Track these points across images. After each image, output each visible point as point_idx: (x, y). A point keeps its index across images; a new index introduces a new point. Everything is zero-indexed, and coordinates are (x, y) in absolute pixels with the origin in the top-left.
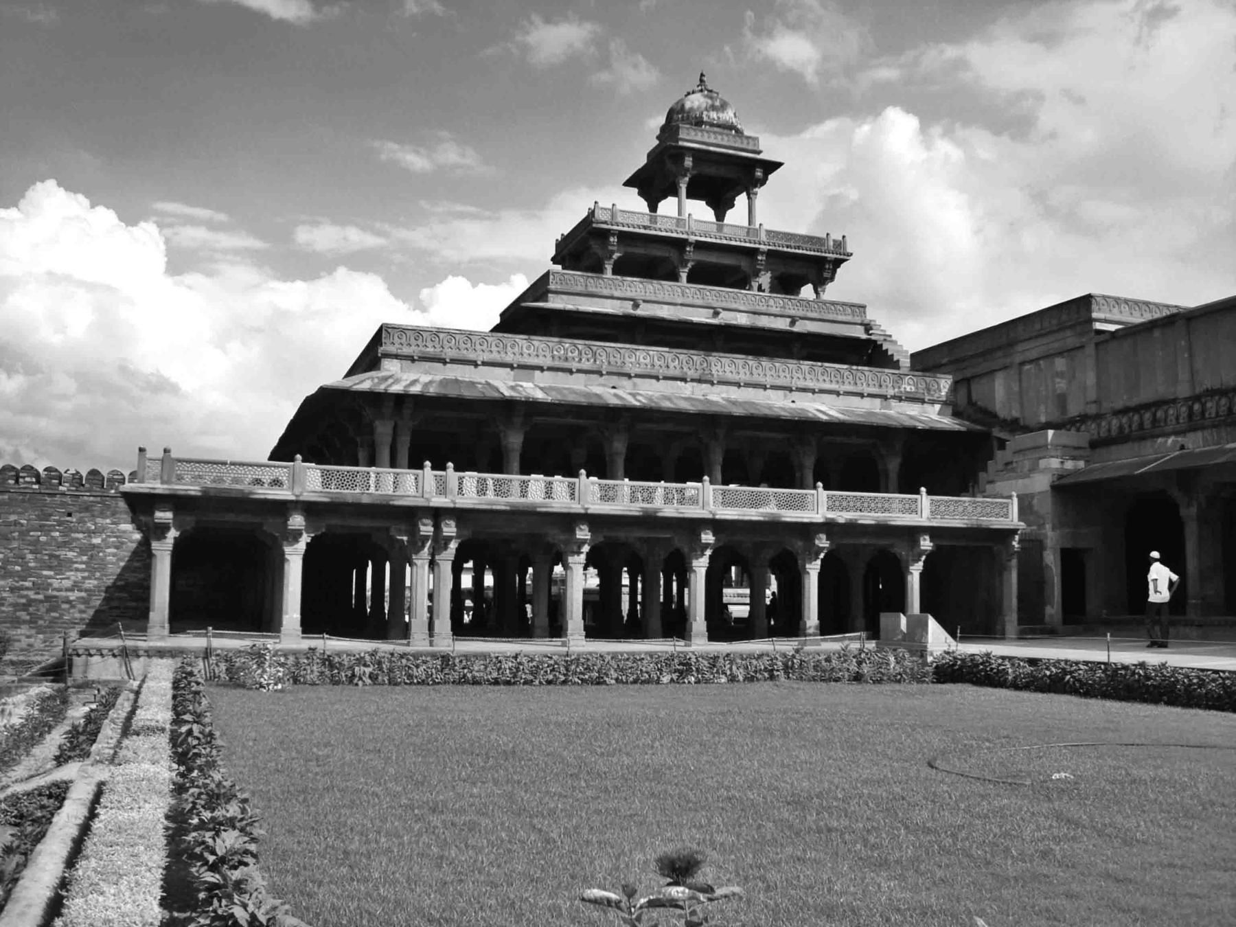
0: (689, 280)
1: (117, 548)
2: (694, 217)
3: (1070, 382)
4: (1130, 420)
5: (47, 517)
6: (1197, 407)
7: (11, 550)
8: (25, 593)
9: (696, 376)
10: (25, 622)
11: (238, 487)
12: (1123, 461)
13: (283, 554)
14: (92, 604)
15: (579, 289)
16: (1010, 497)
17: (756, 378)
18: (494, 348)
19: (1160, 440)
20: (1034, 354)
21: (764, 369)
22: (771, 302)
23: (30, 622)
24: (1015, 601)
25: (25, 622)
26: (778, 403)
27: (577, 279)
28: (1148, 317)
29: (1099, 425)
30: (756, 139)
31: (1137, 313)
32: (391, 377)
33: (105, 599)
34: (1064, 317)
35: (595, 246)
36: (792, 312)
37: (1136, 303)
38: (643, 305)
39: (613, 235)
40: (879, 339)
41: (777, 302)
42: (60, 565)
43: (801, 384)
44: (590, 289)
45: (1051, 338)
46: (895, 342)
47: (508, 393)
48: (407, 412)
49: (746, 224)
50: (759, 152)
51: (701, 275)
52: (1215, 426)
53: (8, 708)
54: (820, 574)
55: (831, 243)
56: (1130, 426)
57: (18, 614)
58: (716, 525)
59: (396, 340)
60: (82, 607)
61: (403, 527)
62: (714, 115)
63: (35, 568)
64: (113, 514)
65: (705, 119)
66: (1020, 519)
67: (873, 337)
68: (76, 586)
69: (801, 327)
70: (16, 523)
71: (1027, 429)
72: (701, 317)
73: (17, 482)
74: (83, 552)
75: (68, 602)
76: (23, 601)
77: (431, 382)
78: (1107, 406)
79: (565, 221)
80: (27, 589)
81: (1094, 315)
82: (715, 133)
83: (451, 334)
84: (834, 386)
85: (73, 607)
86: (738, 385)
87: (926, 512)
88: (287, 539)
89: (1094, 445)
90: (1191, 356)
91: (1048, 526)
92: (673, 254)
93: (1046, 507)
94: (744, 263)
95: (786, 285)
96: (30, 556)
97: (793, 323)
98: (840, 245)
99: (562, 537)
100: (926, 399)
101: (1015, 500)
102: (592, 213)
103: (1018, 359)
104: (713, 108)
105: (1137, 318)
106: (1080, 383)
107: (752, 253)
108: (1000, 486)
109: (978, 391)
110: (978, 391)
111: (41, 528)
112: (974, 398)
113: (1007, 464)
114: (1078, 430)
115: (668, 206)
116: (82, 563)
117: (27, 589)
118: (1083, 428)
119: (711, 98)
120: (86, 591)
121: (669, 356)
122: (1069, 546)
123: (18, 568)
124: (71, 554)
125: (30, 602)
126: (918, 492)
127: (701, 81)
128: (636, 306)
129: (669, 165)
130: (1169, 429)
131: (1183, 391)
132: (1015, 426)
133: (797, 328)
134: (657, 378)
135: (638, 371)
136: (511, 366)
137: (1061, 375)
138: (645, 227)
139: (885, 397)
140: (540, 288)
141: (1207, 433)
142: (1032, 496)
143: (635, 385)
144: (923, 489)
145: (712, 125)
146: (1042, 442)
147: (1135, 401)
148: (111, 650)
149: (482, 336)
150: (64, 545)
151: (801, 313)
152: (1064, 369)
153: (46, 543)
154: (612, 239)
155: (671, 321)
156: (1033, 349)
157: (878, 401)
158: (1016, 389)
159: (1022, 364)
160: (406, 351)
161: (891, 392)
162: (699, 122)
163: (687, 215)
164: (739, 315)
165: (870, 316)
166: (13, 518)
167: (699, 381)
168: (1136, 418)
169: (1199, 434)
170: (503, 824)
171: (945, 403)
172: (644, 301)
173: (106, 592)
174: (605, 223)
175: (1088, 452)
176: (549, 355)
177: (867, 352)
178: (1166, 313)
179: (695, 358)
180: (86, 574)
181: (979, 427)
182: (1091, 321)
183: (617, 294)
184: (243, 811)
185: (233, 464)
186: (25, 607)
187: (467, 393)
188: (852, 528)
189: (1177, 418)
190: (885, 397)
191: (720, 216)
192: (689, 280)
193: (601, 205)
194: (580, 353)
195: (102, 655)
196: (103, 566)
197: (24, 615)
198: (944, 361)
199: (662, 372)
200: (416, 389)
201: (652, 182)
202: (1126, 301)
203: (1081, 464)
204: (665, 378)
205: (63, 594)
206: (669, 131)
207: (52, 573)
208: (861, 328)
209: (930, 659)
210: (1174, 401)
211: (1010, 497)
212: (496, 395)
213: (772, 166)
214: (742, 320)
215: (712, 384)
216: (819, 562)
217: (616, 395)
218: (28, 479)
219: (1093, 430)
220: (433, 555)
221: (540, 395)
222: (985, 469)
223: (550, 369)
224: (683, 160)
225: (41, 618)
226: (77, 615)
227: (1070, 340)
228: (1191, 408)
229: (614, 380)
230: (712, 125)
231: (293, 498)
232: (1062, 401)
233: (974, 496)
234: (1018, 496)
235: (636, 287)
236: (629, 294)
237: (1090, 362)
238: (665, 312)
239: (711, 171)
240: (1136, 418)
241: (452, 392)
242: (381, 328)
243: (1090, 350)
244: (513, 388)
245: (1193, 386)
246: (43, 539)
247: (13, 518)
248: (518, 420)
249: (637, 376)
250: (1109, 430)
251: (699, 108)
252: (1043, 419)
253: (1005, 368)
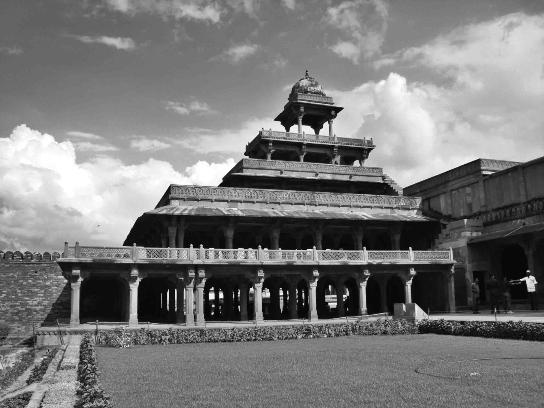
0: (305, 161)
1: (57, 286)
2: (306, 133)
3: (473, 198)
4: (500, 213)
5: (26, 273)
6: (529, 206)
7: (11, 289)
8: (17, 307)
9: (309, 202)
10: (17, 321)
11: (109, 258)
12: (498, 231)
13: (129, 287)
14: (47, 311)
15: (257, 166)
16: (449, 250)
17: (335, 202)
18: (220, 194)
19: (514, 221)
20: (456, 186)
21: (338, 198)
22: (341, 169)
23: (19, 320)
24: (454, 296)
25: (17, 321)
26: (345, 213)
27: (256, 162)
28: (505, 168)
29: (487, 216)
30: (331, 98)
31: (500, 166)
32: (175, 208)
33: (52, 309)
34: (469, 170)
35: (263, 148)
36: (350, 173)
37: (500, 161)
38: (284, 172)
39: (271, 142)
40: (389, 183)
41: (343, 169)
42: (32, 295)
43: (355, 204)
44: (261, 166)
46: (396, 184)
47: (226, 213)
48: (182, 223)
49: (329, 135)
50: (333, 104)
51: (309, 158)
52: (538, 214)
53: (8, 359)
54: (366, 288)
55: (366, 142)
56: (501, 216)
57: (14, 317)
58: (319, 268)
59: (177, 192)
60: (42, 313)
61: (182, 274)
62: (312, 88)
63: (20, 296)
64: (55, 271)
65: (309, 90)
66: (454, 259)
67: (386, 182)
68: (39, 304)
69: (355, 179)
70: (13, 277)
71: (455, 219)
72: (310, 176)
73: (13, 259)
74: (42, 289)
75: (36, 311)
76: (16, 311)
77: (192, 209)
78: (490, 208)
79: (250, 137)
80: (18, 306)
81: (482, 168)
82: (313, 96)
83: (201, 188)
84: (369, 204)
85: (38, 313)
86: (327, 205)
87: (412, 258)
88: (131, 281)
89: (486, 225)
90: (525, 184)
91: (467, 262)
92: (297, 150)
93: (465, 253)
94: (328, 152)
95: (347, 161)
96: (19, 291)
97: (351, 177)
98: (370, 142)
99: (252, 275)
100: (411, 208)
101: (451, 251)
102: (261, 133)
103: (450, 188)
104: (312, 85)
105: (501, 169)
106: (477, 197)
107: (331, 148)
108: (445, 245)
109: (433, 204)
110: (433, 204)
111: (23, 279)
112: (431, 207)
113: (447, 235)
114: (478, 218)
115: (294, 129)
116: (42, 293)
117: (18, 306)
118: (480, 217)
119: (311, 81)
120: (44, 306)
121: (297, 194)
122: (477, 270)
123: (13, 297)
124: (37, 290)
125: (19, 312)
126: (408, 249)
127: (307, 74)
128: (282, 173)
129: (294, 111)
130: (518, 216)
131: (523, 199)
132: (450, 218)
133: (352, 180)
134: (292, 204)
135: (284, 201)
136: (227, 201)
137: (469, 195)
138: (284, 138)
139: (392, 208)
140: (239, 167)
141: (534, 217)
142: (459, 249)
143: (282, 207)
144: (410, 248)
145: (312, 93)
146: (462, 225)
147: (503, 205)
148: (54, 332)
149: (214, 188)
150: (34, 286)
151: (354, 173)
152: (470, 192)
153: (26, 285)
154: (270, 144)
155: (297, 179)
156: (455, 184)
157: (389, 210)
158: (449, 201)
159: (452, 190)
160: (181, 196)
161: (395, 206)
162: (306, 92)
163: (303, 132)
164: (327, 175)
165: (384, 173)
166: (11, 274)
167: (310, 204)
168: (503, 212)
169: (531, 218)
170: (224, 404)
171: (418, 210)
172: (285, 170)
173: (53, 306)
174: (267, 137)
175: (482, 228)
176: (244, 196)
177: (384, 189)
178: (513, 165)
179: (308, 194)
180: (44, 298)
181: (434, 220)
182: (481, 170)
183: (273, 168)
184: (106, 403)
185: (106, 248)
186: (17, 314)
187: (209, 214)
188: (380, 266)
189: (521, 212)
190: (392, 208)
191: (317, 132)
192: (305, 160)
193: (265, 129)
194: (257, 194)
195: (50, 334)
196: (51, 294)
197: (16, 318)
198: (418, 191)
199: (294, 201)
200: (186, 213)
201: (287, 118)
202: (496, 161)
203: (480, 234)
204: (295, 204)
205: (34, 307)
206: (293, 95)
207: (28, 298)
208: (381, 178)
209: (417, 323)
210: (518, 204)
211: (449, 250)
212: (221, 214)
213: (339, 109)
214: (329, 177)
215: (316, 205)
216: (366, 282)
217: (274, 212)
218: (17, 257)
219: (484, 219)
220: (195, 286)
221: (240, 213)
222: (438, 238)
223: (245, 202)
224: (300, 109)
225: (24, 318)
226: (40, 317)
227: (472, 179)
228: (526, 207)
229: (273, 205)
230: (312, 93)
231: (133, 262)
232: (470, 206)
233: (433, 250)
234: (453, 249)
235: (281, 164)
236: (278, 168)
237: (481, 189)
238: (294, 175)
239: (312, 112)
240: (503, 212)
241: (202, 213)
242: (170, 187)
243: (481, 183)
244: (228, 211)
245: (527, 198)
246: (24, 283)
247: (11, 274)
248: (231, 225)
249: (283, 203)
250: (491, 218)
251: (306, 86)
252: (462, 214)
253: (444, 193)
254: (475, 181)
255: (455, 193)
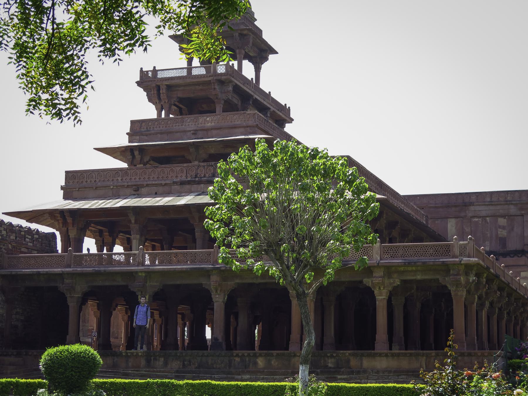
20: (484, 213)
45: (499, 207)
103: (470, 214)
137: (504, 228)
152: (506, 225)
232: (503, 241)
253: (456, 217)
254: (519, 213)
255: (477, 222)
